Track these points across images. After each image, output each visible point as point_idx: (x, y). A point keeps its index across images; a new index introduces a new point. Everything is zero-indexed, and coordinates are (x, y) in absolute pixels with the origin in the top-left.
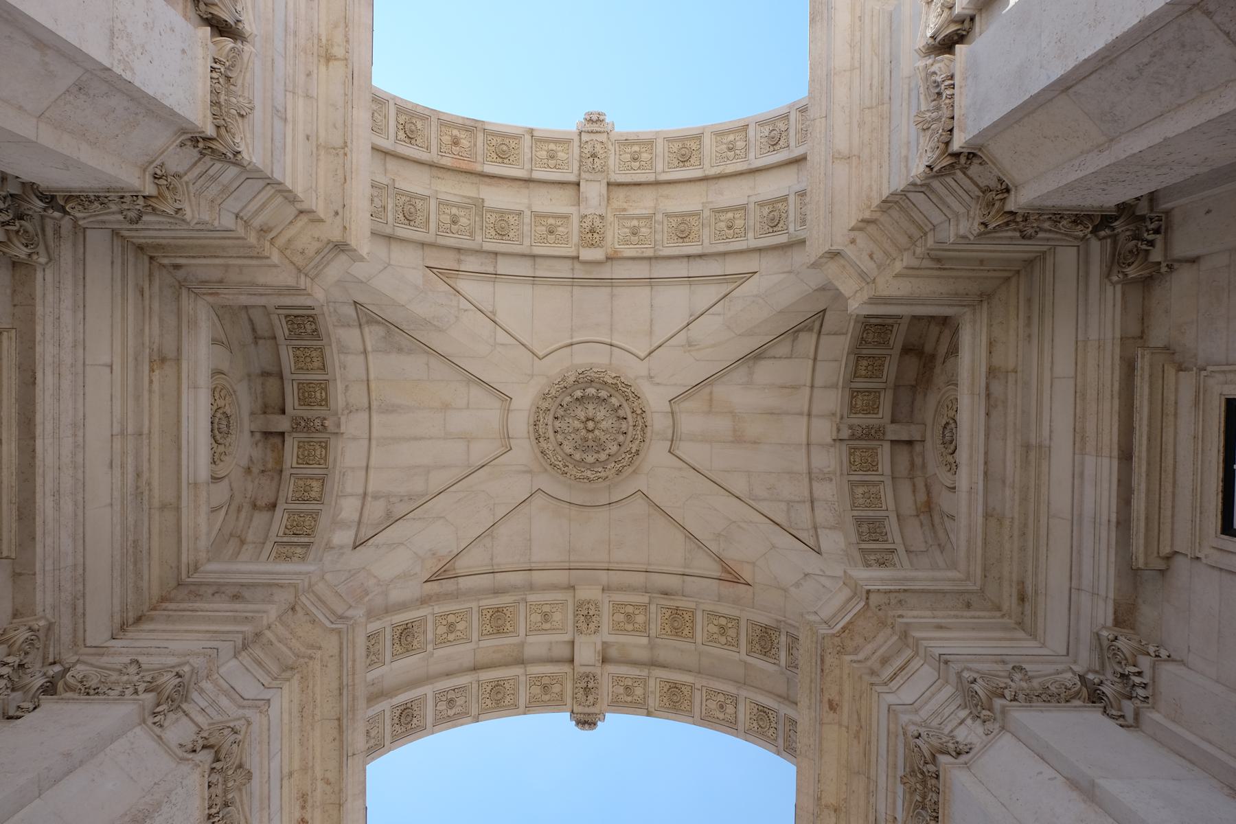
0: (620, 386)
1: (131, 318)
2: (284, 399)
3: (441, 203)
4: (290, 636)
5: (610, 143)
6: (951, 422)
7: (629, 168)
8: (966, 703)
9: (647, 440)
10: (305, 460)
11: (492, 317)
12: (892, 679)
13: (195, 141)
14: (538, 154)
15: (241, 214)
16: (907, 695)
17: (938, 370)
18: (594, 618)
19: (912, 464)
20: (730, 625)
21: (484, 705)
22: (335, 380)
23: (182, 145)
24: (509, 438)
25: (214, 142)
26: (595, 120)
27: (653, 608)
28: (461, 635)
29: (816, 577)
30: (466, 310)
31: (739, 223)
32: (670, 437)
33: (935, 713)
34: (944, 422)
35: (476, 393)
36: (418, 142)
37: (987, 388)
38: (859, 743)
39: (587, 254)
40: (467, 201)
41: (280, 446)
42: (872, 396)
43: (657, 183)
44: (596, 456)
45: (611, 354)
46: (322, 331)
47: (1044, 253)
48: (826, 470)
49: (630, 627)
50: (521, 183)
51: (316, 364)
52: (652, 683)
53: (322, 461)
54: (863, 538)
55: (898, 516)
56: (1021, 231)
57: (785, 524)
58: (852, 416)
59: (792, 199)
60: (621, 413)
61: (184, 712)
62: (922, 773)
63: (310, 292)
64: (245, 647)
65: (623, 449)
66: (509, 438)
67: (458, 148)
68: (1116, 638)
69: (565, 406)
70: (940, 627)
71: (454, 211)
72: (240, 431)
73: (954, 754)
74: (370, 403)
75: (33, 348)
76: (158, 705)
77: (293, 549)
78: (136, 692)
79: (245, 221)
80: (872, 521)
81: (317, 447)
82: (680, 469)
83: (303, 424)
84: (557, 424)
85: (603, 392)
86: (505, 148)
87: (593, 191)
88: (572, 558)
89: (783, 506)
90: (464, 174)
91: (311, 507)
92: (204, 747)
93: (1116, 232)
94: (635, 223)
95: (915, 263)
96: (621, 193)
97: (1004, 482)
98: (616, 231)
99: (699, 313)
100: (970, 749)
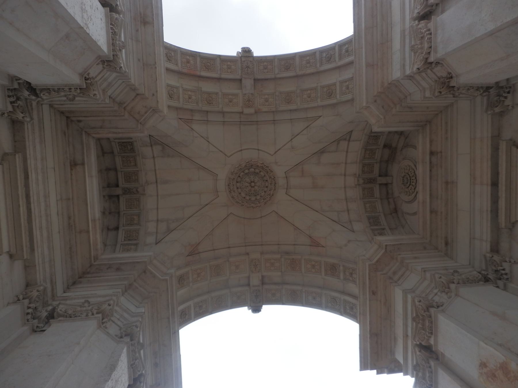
3: (185, 90)
6: (407, 175)
13: (103, 62)
15: (112, 96)
19: (388, 193)
20: (316, 264)
24: (217, 192)
26: (247, 52)
30: (196, 137)
39: (247, 111)
43: (275, 79)
56: (453, 94)
59: (338, 84)
60: (265, 178)
61: (112, 321)
64: (126, 291)
68: (493, 256)
70: (415, 258)
71: (190, 93)
73: (436, 307)
76: (103, 319)
78: (93, 314)
84: (238, 184)
86: (209, 64)
87: (248, 83)
92: (126, 335)
93: (490, 93)
94: (266, 96)
100: (443, 304)
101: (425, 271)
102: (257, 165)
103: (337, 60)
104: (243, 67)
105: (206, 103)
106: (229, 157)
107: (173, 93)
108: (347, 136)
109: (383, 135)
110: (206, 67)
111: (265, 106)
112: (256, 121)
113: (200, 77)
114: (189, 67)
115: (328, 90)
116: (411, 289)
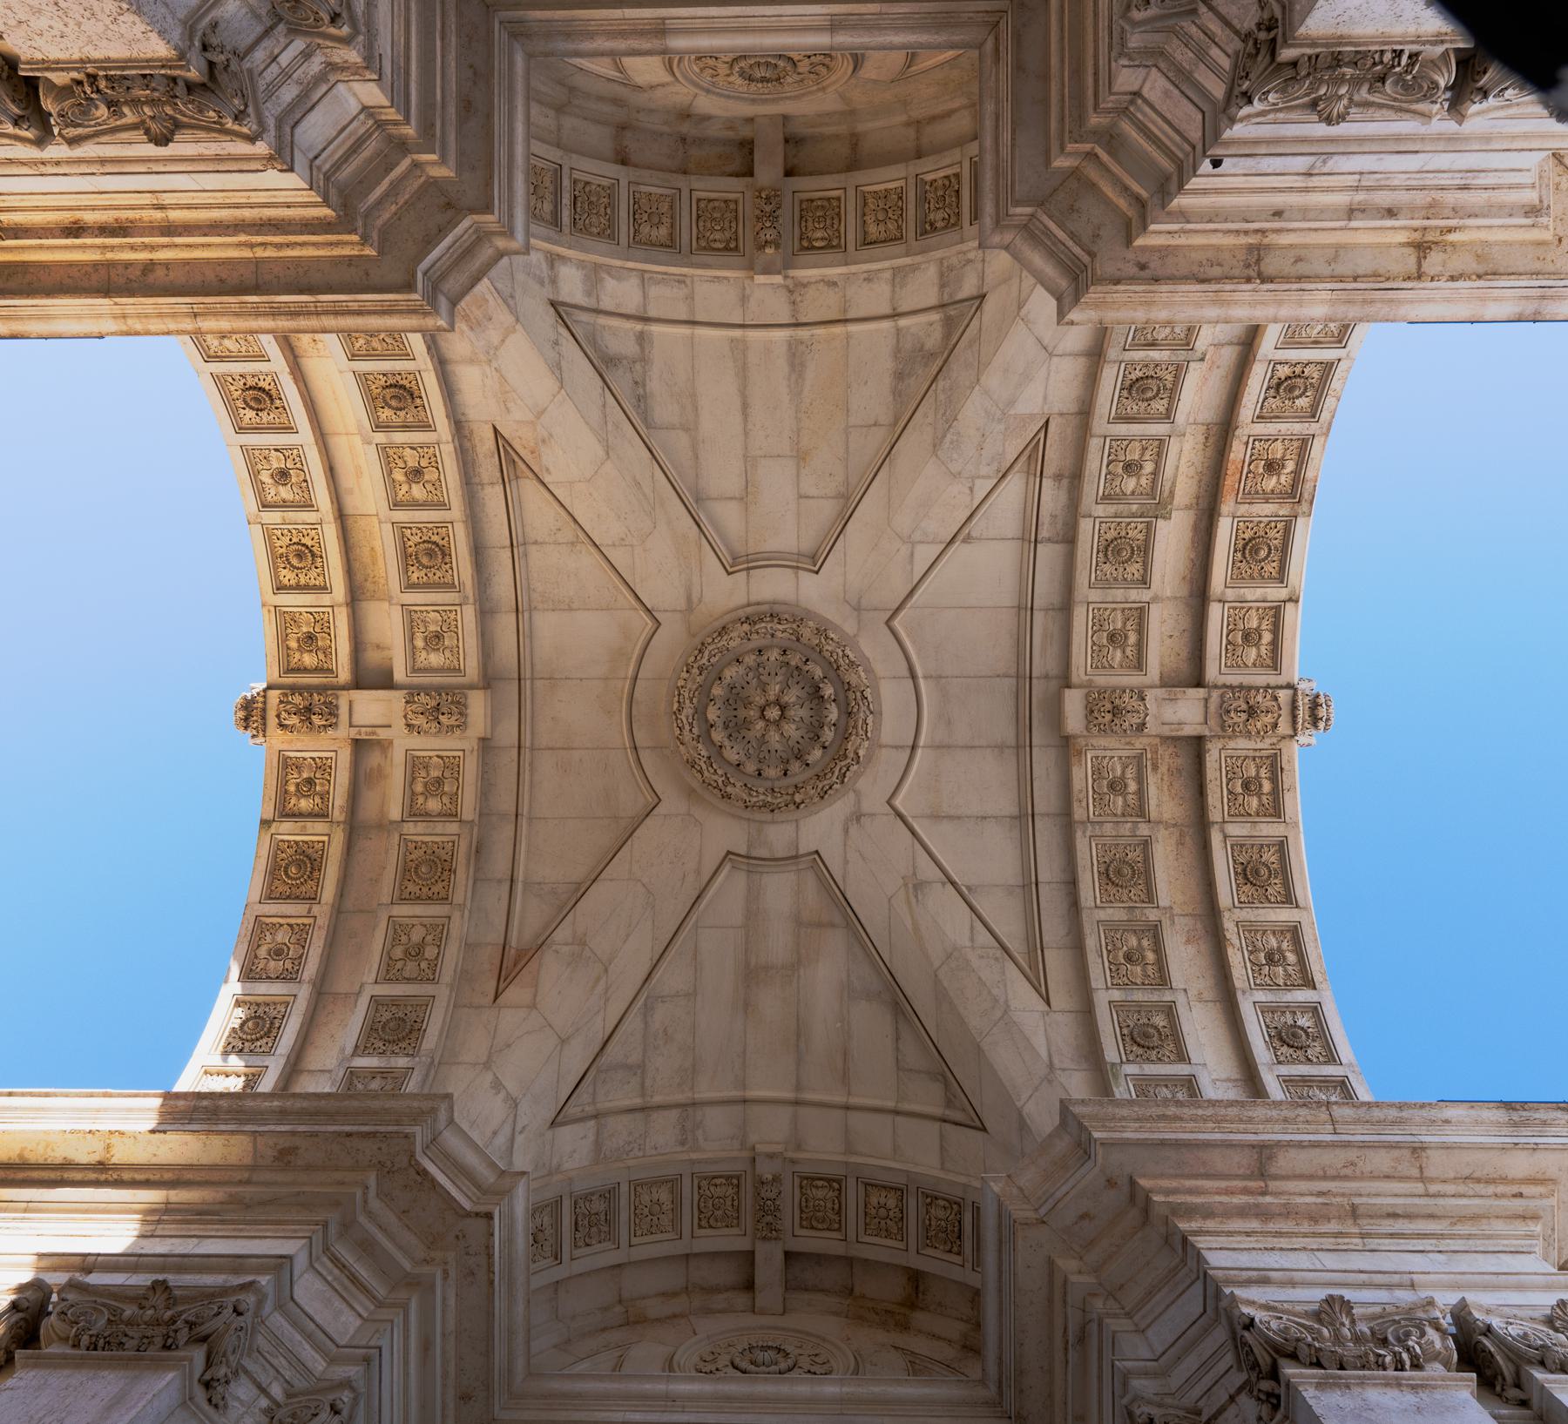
0: (843, 763)
2: (811, 174)
3: (1161, 444)
4: (401, 202)
5: (1275, 740)
6: (790, 1362)
8: (295, 1396)
9: (747, 814)
10: (705, 211)
11: (961, 537)
12: (335, 1260)
14: (1253, 613)
16: (309, 1290)
18: (435, 724)
21: (279, 533)
22: (846, 264)
24: (748, 569)
27: (453, 828)
28: (403, 492)
29: (510, 1120)
30: (971, 489)
32: (754, 854)
33: (277, 1342)
34: (789, 1349)
35: (827, 510)
36: (1271, 400)
38: (222, 1203)
39: (1074, 703)
40: (1166, 494)
42: (833, 1217)
44: (720, 723)
45: (896, 747)
46: (933, 239)
48: (699, 1133)
49: (419, 788)
52: (320, 827)
53: (703, 243)
54: (581, 1203)
55: (619, 1266)
57: (604, 1060)
58: (797, 1181)
60: (795, 767)
62: (173, 1321)
65: (730, 771)
66: (748, 569)
67: (1261, 470)
69: (807, 668)
70: (426, 1346)
71: (1149, 467)
73: (207, 1377)
77: (549, 197)
80: (610, 1219)
81: (728, 235)
82: (698, 872)
83: (768, 208)
84: (774, 655)
85: (832, 734)
86: (1263, 554)
88: (538, 683)
89: (635, 1058)
91: (624, 228)
94: (1132, 787)
96: (1183, 761)
98: (1120, 753)
99: (974, 903)
100: (216, 1406)
101: (370, 1359)
103: (1285, 1070)
104: (1253, 692)
105: (1109, 536)
106: (888, 623)
108: (964, 1110)
110: (1250, 540)
111: (1094, 780)
114: (1249, 472)
115: (1158, 1031)
116: (292, 1298)
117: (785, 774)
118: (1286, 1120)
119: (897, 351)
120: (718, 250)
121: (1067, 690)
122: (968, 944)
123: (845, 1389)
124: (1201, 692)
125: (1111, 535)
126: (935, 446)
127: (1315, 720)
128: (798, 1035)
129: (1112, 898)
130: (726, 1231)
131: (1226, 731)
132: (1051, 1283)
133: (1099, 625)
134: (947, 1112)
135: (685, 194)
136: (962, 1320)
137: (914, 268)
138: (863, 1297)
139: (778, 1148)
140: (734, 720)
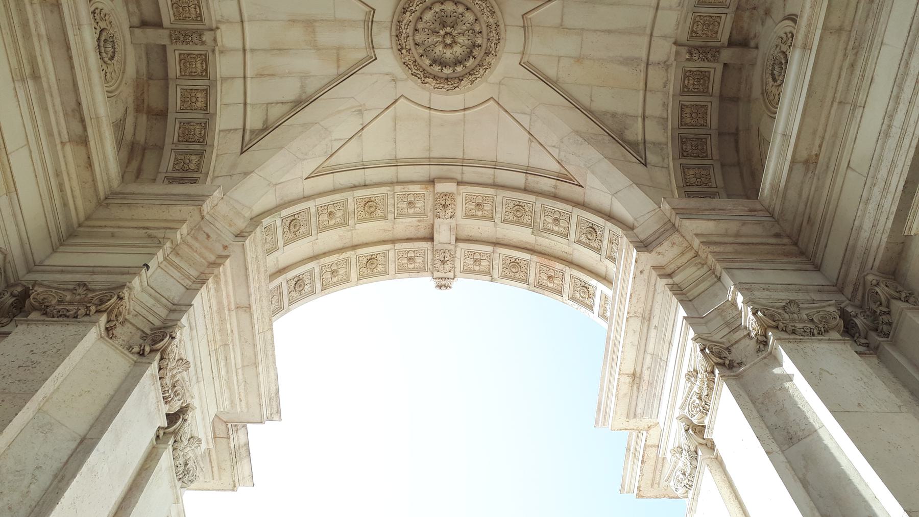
0: (422, 76)
1: (827, 186)
5: (431, 270)
7: (416, 252)
10: (712, 22)
11: (531, 138)
17: (130, 100)
23: (740, 364)
24: (524, 27)
25: (716, 361)
30: (554, 146)
31: (325, 217)
34: (115, 58)
35: (551, 72)
37: (85, 128)
40: (543, 234)
41: (734, 32)
43: (393, 241)
45: (430, 100)
47: (61, 245)
50: (502, 242)
51: (688, 111)
56: (88, 289)
63: (673, 212)
65: (418, 14)
67: (549, 274)
71: (556, 229)
72: (766, 54)
74: (647, 68)
75: (899, 210)
79: (714, 273)
81: (700, 32)
84: (479, 41)
85: (437, 70)
86: (514, 270)
90: (547, 253)
94: (411, 211)
95: (169, 234)
96: (422, 232)
97: (49, 39)
99: (353, 140)
102: (437, 80)
104: (452, 262)
106: (492, 97)
107: (589, 236)
109: (173, 144)
111: (413, 195)
112: (431, 166)
113: (532, 251)
114: (550, 269)
117: (416, 44)
118: (263, 314)
119: (626, 115)
120: (693, 27)
121: (456, 184)
122: (333, 138)
123: (104, 119)
124: (453, 241)
125: (527, 209)
126: (577, 131)
127: (440, 287)
128: (280, 50)
129: (358, 204)
130: (171, 13)
131: (434, 251)
132: (174, 221)
133: (485, 198)
134: (248, 132)
135: (726, 11)
136: (146, 140)
137: (665, 129)
138: (149, 85)
139: (219, 43)
140: (445, 15)
